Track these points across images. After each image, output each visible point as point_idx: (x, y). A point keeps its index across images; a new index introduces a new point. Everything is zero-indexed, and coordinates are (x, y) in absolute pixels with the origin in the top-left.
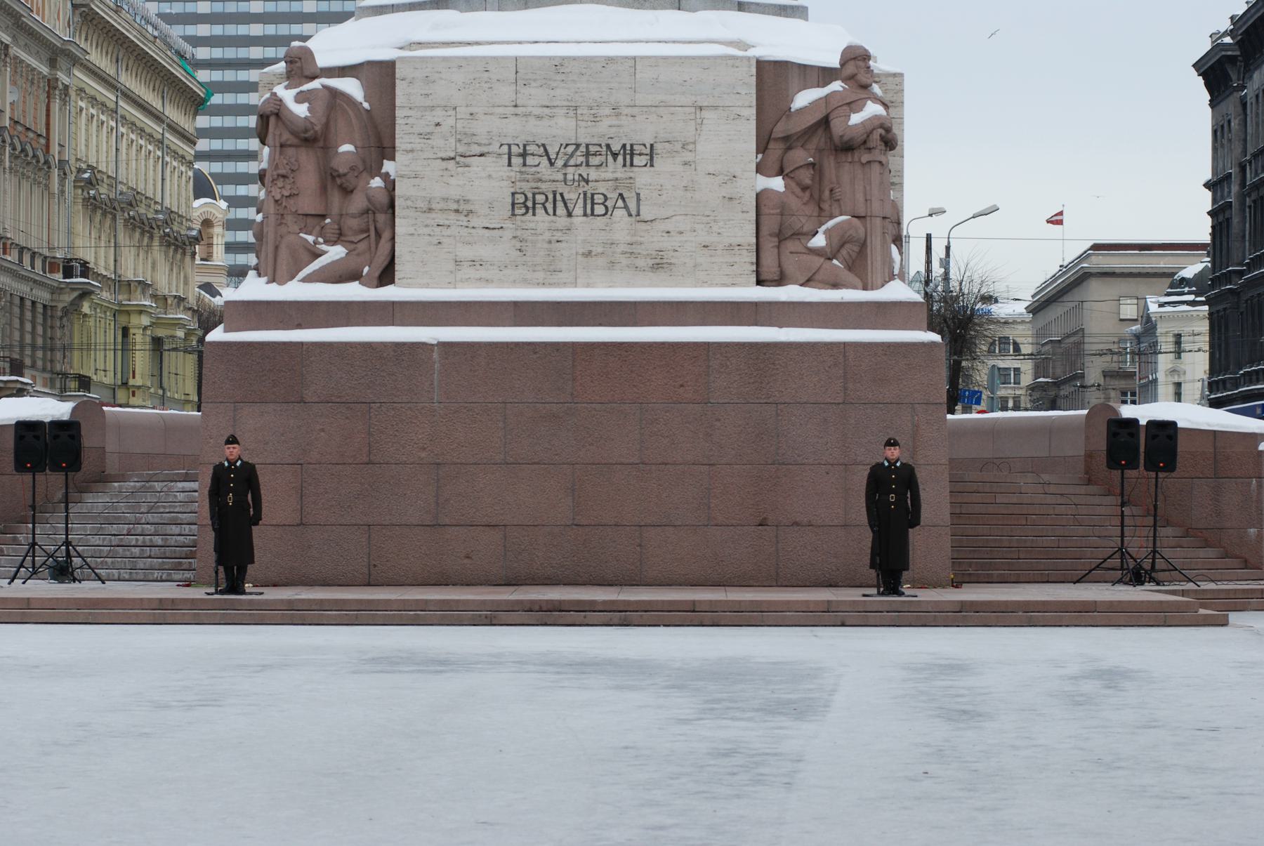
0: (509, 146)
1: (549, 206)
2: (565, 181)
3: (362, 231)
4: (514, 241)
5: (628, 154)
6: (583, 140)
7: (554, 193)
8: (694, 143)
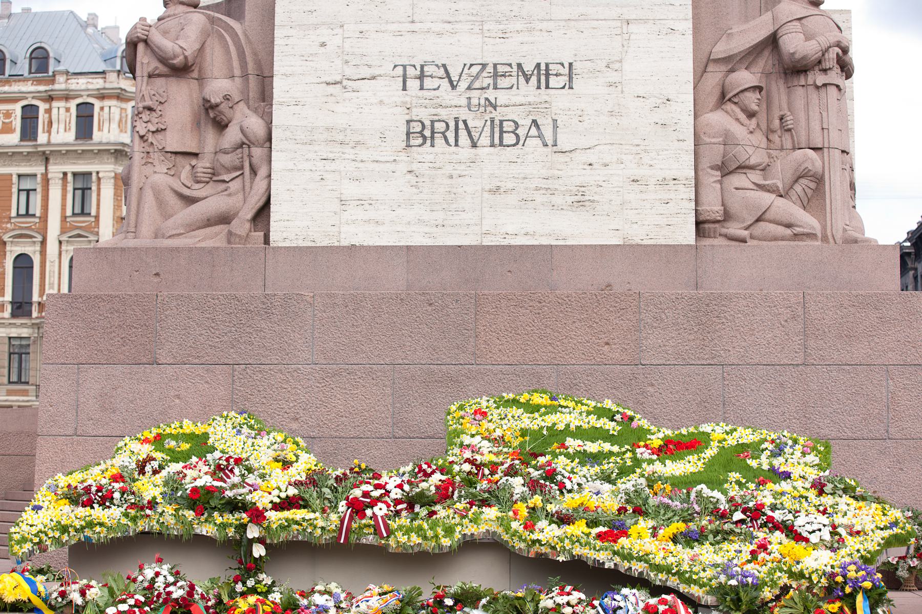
0: (404, 67)
1: (451, 135)
3: (236, 169)
4: (409, 176)
5: (543, 74)
6: (490, 60)
7: (457, 120)
8: (621, 61)
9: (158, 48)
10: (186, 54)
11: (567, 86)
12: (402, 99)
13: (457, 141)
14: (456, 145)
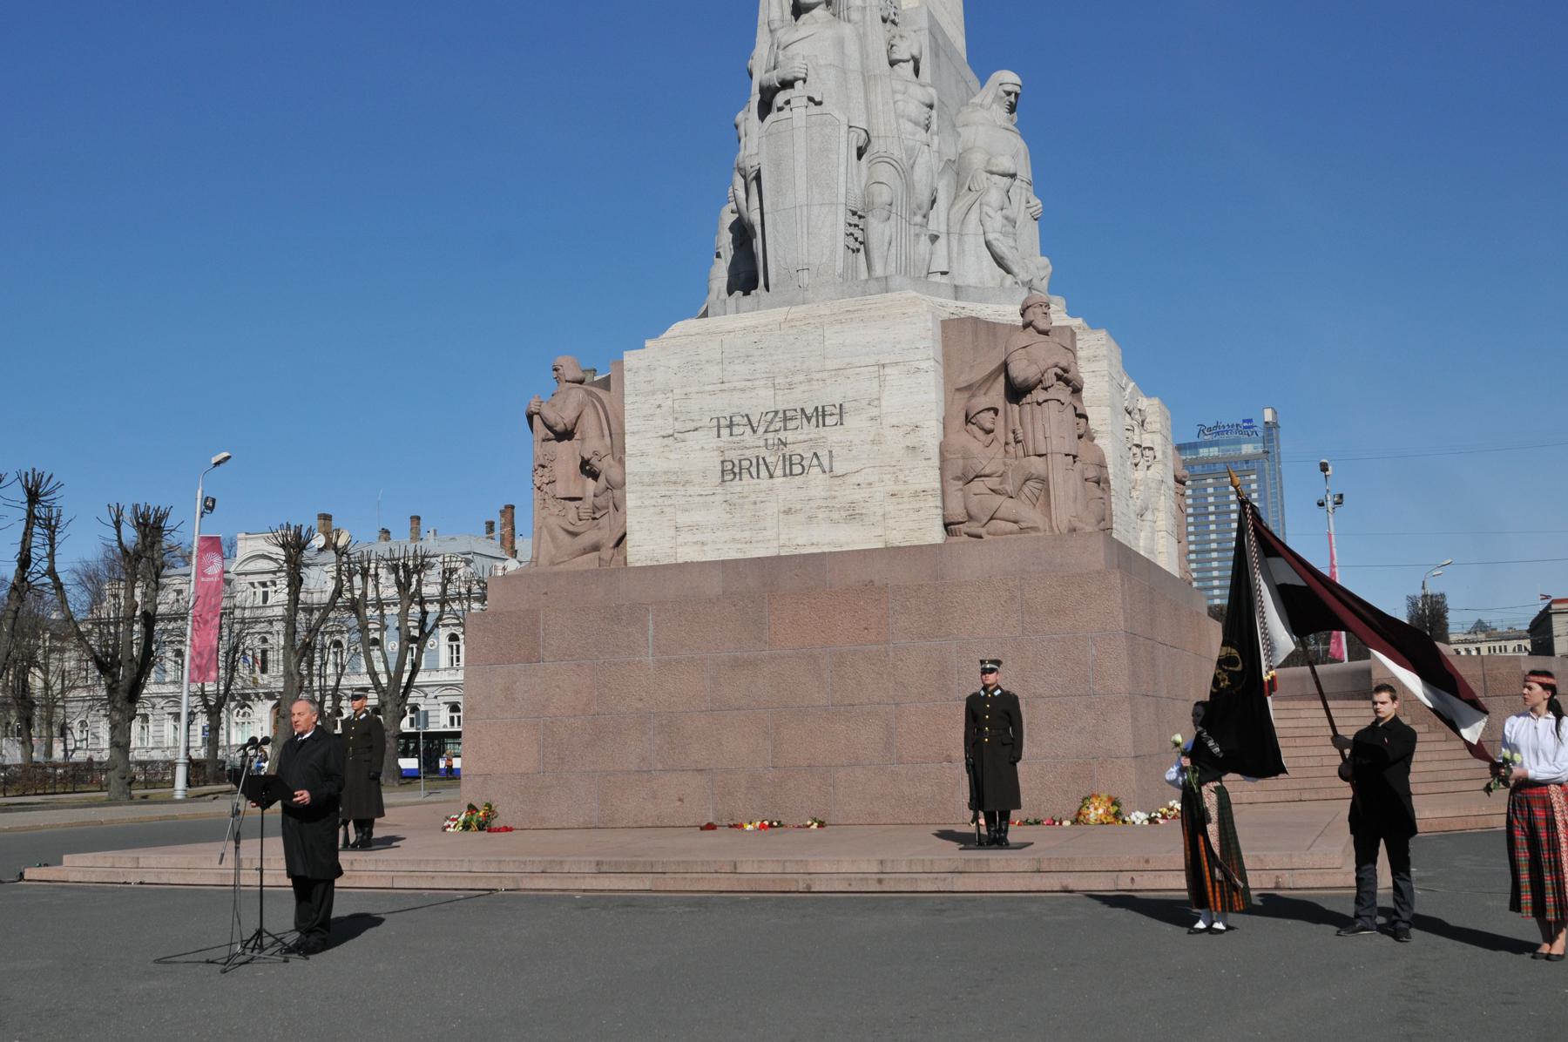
5: (820, 415)
6: (781, 408)
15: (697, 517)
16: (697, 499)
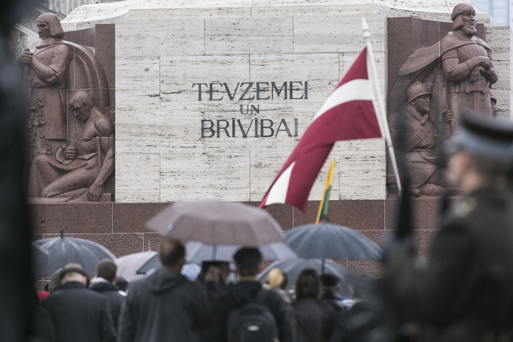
0: (200, 85)
1: (230, 130)
2: (241, 111)
4: (204, 156)
5: (288, 89)
6: (255, 80)
7: (234, 120)
9: (38, 69)
10: (58, 75)
11: (304, 97)
12: (199, 106)
13: (234, 133)
14: (234, 136)
15: (177, 165)
16: (179, 150)
